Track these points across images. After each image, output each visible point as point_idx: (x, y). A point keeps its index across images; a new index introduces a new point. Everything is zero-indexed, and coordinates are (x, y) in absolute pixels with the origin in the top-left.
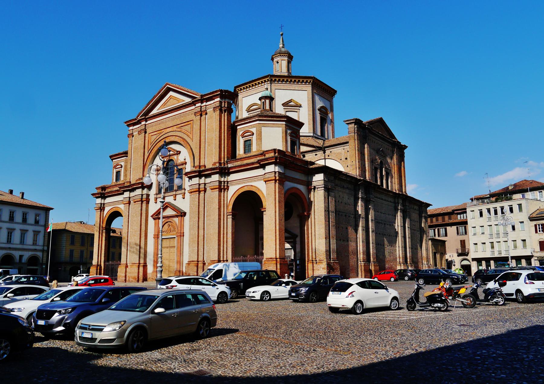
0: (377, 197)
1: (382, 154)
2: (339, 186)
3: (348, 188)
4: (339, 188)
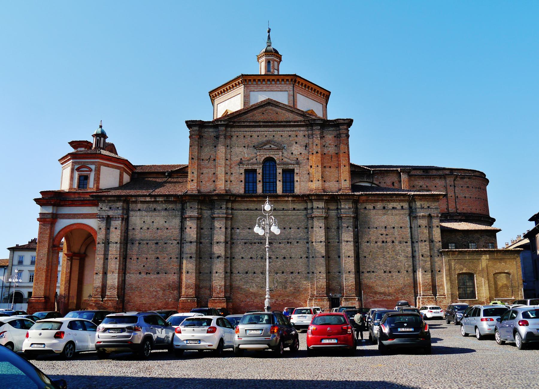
0: (248, 209)
1: (272, 146)
2: (142, 211)
3: (166, 209)
4: (143, 212)
